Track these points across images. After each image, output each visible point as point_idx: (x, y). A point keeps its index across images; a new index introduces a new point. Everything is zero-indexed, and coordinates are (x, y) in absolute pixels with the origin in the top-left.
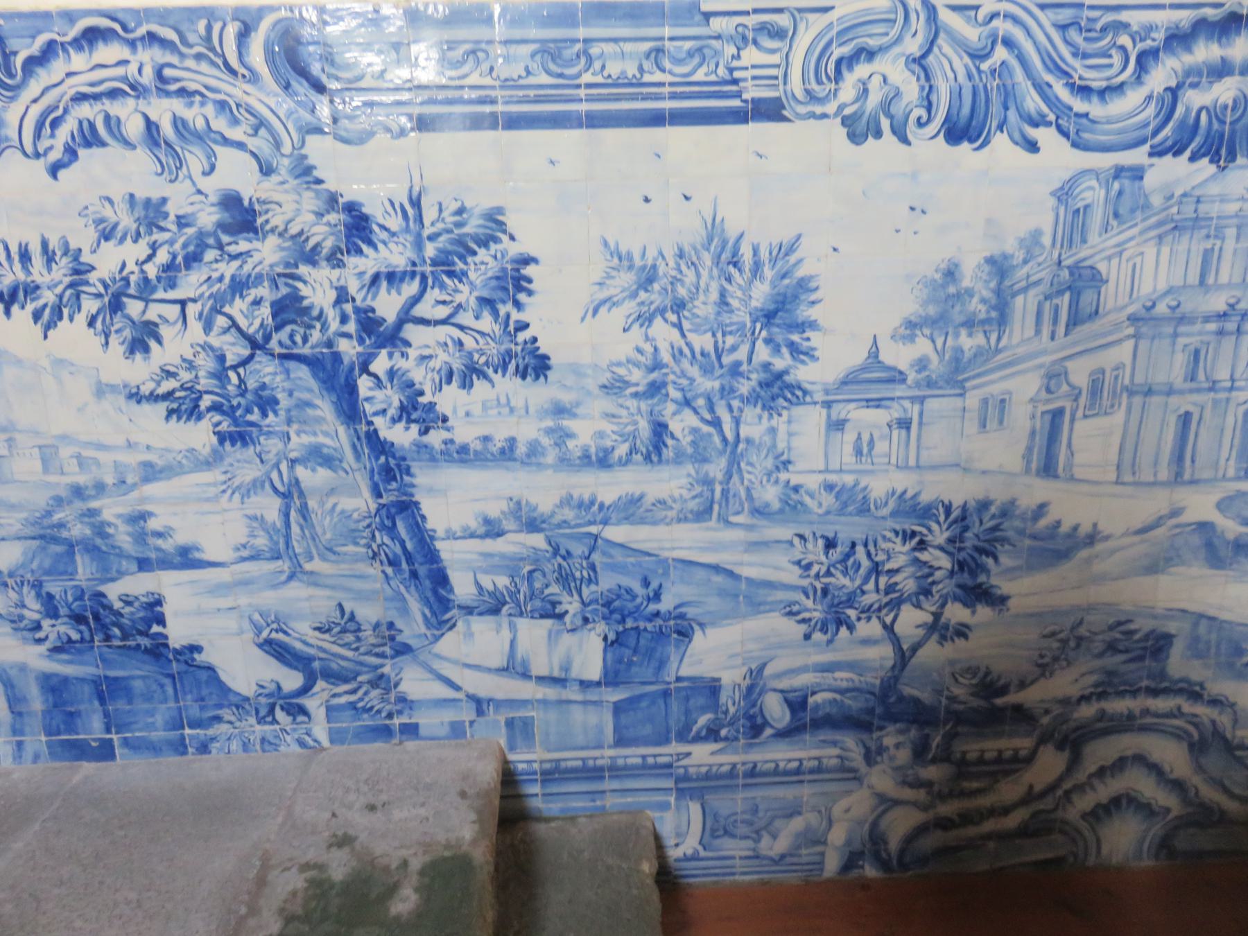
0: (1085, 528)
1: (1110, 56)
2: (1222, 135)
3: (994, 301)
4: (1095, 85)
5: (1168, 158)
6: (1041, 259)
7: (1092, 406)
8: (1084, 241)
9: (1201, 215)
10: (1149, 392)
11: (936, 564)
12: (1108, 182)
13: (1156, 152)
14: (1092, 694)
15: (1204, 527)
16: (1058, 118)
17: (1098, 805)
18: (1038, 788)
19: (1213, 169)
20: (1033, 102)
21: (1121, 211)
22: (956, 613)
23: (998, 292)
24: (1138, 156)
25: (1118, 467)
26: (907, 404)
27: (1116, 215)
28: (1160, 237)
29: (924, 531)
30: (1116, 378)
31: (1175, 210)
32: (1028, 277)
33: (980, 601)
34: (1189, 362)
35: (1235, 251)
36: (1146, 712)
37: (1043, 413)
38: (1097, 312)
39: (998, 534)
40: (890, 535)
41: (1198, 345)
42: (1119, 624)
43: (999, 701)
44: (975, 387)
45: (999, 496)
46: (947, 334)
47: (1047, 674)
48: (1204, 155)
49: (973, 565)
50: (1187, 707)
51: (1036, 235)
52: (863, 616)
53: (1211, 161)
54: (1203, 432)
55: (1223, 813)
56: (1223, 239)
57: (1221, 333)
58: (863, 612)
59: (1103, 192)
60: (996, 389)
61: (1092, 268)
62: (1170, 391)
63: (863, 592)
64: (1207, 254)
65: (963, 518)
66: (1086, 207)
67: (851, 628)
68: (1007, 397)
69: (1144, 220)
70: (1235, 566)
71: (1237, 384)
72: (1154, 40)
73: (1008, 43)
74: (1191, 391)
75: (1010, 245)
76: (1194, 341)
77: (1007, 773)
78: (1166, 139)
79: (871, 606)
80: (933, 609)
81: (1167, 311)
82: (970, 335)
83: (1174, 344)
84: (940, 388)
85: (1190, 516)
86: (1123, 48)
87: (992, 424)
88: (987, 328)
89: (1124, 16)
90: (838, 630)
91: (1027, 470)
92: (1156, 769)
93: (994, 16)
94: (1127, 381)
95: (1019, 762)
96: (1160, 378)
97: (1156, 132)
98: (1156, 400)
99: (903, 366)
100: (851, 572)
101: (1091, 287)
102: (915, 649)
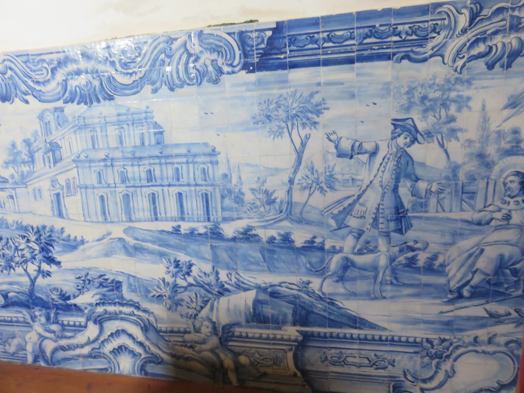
0: (79, 238)
1: (43, 71)
2: (86, 95)
3: (29, 154)
4: (40, 80)
5: (70, 104)
6: (39, 140)
7: (68, 193)
8: (51, 134)
9: (86, 123)
10: (86, 188)
11: (35, 248)
12: (53, 113)
13: (66, 102)
14: (100, 303)
15: (120, 239)
16: (32, 92)
17: (114, 349)
18: (92, 339)
19: (86, 107)
20: (23, 87)
21: (60, 123)
22: (45, 267)
23: (29, 151)
24: (60, 104)
25: (84, 216)
26: (10, 190)
27: (59, 124)
28: (75, 132)
29: (28, 236)
30: (74, 182)
31: (77, 122)
32: (37, 146)
33: (52, 263)
34: (97, 177)
35: (102, 136)
36: (121, 312)
37: (54, 194)
38: (61, 158)
39: (51, 238)
40: (18, 236)
41: (99, 170)
42: (102, 276)
43: (69, 302)
44: (31, 185)
45: (48, 224)
46: (18, 166)
47: (82, 293)
48: (82, 102)
49: (46, 249)
50: (136, 312)
51: (36, 132)
52: (17, 265)
53: (85, 104)
54: (109, 202)
55: (162, 359)
56: (96, 132)
57: (106, 166)
58: (16, 264)
59: (53, 117)
60: (37, 185)
61: (56, 143)
62: (94, 188)
63: (15, 257)
64: (92, 138)
65: (38, 231)
66: (49, 122)
67: (14, 269)
68: (40, 188)
69: (68, 125)
70: (136, 256)
71: (117, 185)
72: (54, 64)
73: (11, 69)
74: (101, 188)
75: (29, 136)
76: (97, 169)
77: (80, 331)
78: (67, 97)
79: (18, 262)
80: (38, 264)
81: (85, 158)
82: (25, 166)
83: (90, 170)
84: (19, 185)
85: (113, 236)
86: (46, 68)
87: (38, 198)
88: (29, 164)
89: (43, 57)
90: (10, 270)
91: (54, 215)
92: (130, 336)
93: (4, 60)
94: (78, 184)
95: (81, 328)
96: (89, 183)
97: (63, 95)
98: (90, 191)
99: (7, 177)
100: (10, 249)
101: (57, 150)
102: (36, 278)
